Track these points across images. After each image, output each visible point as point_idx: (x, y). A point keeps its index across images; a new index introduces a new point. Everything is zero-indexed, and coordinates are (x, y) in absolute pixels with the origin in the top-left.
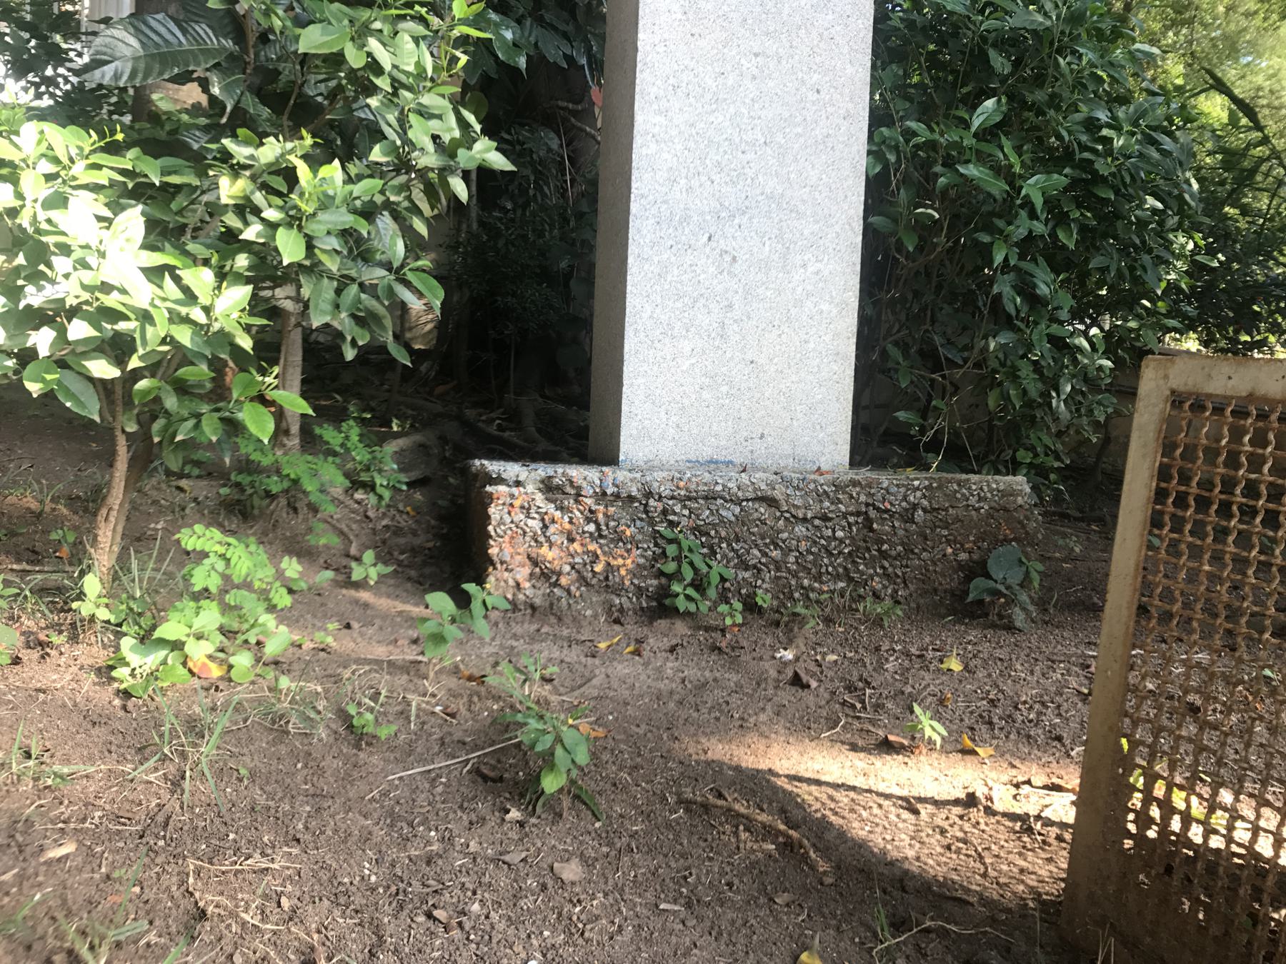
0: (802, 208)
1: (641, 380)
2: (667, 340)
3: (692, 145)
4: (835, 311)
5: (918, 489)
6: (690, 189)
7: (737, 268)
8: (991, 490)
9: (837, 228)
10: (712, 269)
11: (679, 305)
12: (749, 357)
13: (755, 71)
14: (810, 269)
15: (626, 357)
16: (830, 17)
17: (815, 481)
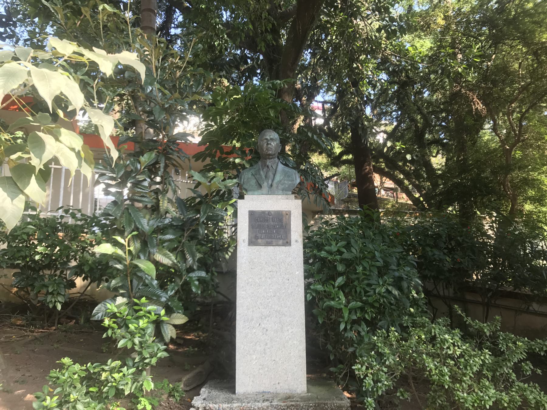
0: (286, 314)
1: (241, 368)
2: (248, 356)
3: (253, 299)
4: (298, 344)
5: (312, 406)
6: (253, 311)
7: (268, 333)
8: (334, 406)
9: (297, 319)
10: (261, 334)
11: (252, 345)
12: (273, 359)
13: (270, 276)
14: (290, 331)
15: (237, 361)
17: (280, 405)
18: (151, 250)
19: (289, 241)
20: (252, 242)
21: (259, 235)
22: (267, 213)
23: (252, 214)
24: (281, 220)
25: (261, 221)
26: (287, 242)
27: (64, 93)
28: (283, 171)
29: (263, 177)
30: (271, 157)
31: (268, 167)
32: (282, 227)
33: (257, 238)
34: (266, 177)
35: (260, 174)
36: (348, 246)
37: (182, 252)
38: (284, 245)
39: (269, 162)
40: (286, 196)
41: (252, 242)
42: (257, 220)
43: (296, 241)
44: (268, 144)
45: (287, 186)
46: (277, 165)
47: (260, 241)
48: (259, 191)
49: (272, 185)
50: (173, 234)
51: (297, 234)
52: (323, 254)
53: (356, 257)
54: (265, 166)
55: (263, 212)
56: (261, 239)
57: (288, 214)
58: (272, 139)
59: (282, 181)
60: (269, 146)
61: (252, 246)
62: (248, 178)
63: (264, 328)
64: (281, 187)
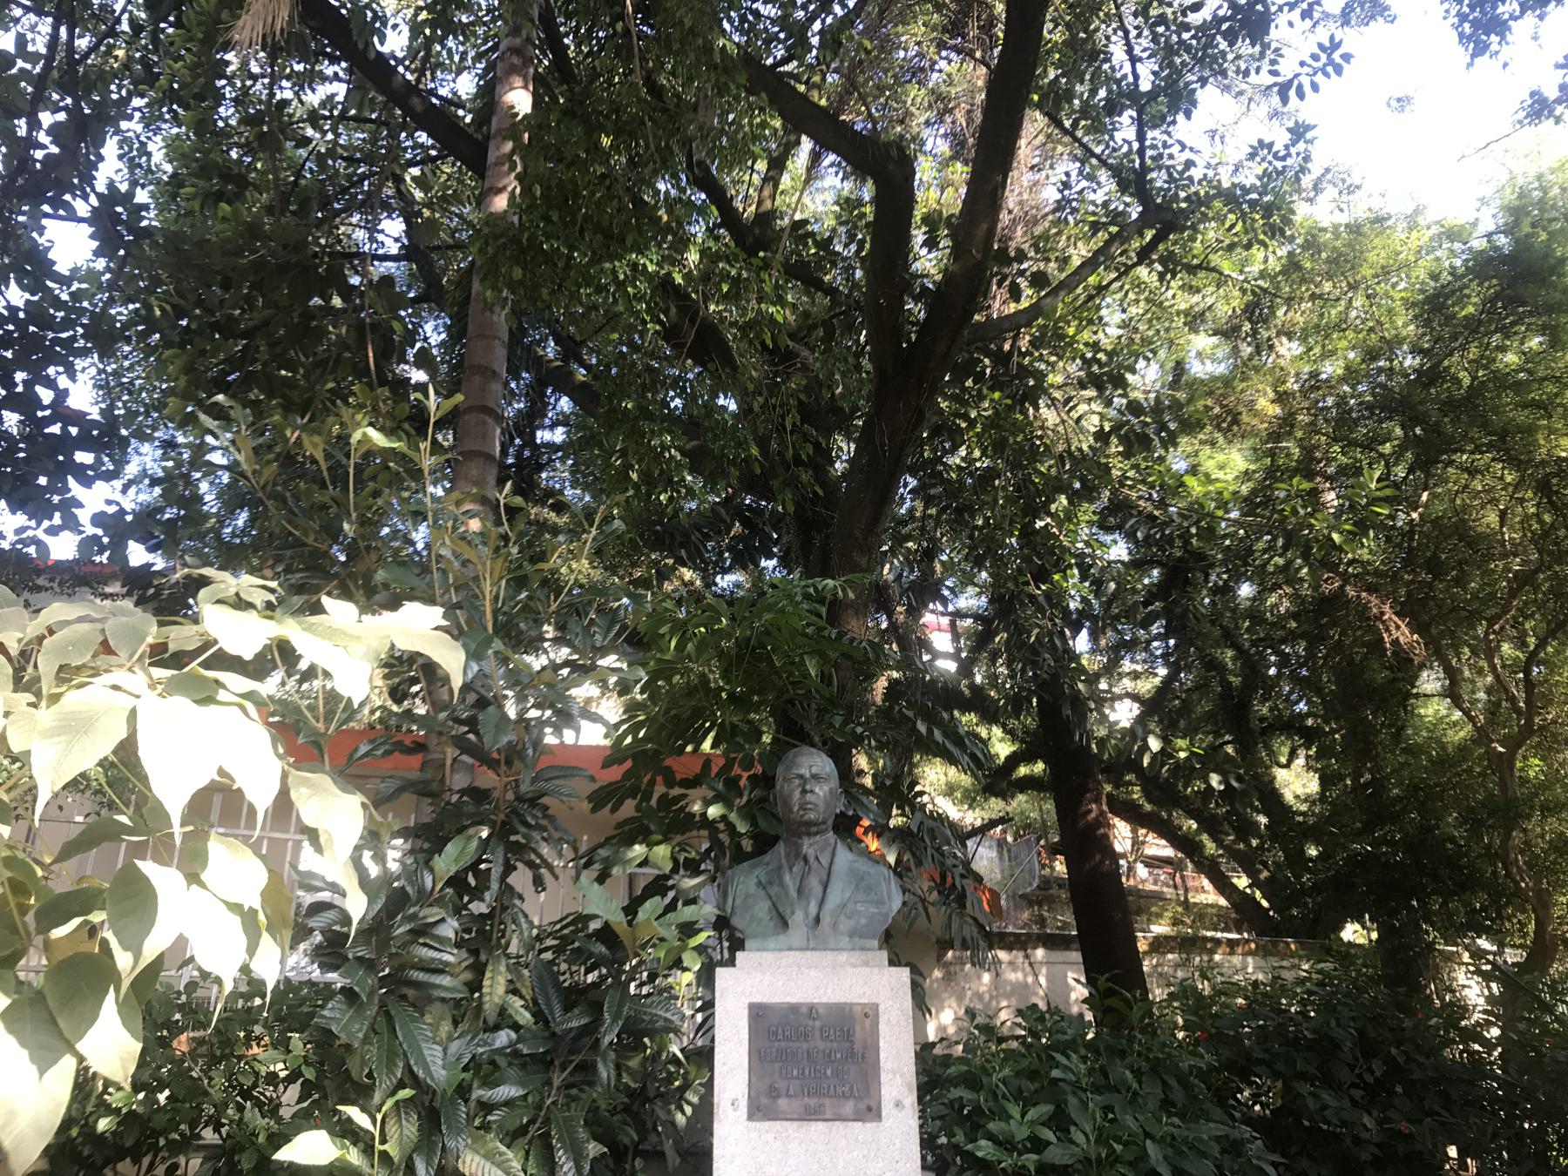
16: (881, 1164)
18: (451, 1144)
19: (874, 1105)
20: (761, 1108)
21: (781, 1085)
22: (804, 1010)
23: (759, 1014)
24: (847, 1035)
25: (786, 1038)
26: (869, 1109)
27: (226, 769)
28: (852, 872)
29: (793, 893)
30: (814, 829)
31: (806, 860)
32: (851, 1055)
33: (773, 1093)
34: (800, 891)
35: (782, 884)
36: (1061, 1122)
37: (546, 1137)
38: (859, 1117)
39: (808, 846)
40: (863, 956)
41: (761, 1108)
42: (776, 1034)
43: (898, 1104)
44: (804, 792)
45: (863, 921)
46: (833, 855)
47: (783, 1103)
48: (782, 938)
49: (817, 920)
50: (521, 1084)
51: (899, 1080)
52: (984, 1149)
53: (1088, 1160)
54: (797, 855)
55: (794, 1008)
56: (788, 1096)
57: (871, 1013)
58: (815, 777)
59: (850, 907)
60: (809, 797)
61: (758, 1120)
62: (747, 896)
64: (846, 924)
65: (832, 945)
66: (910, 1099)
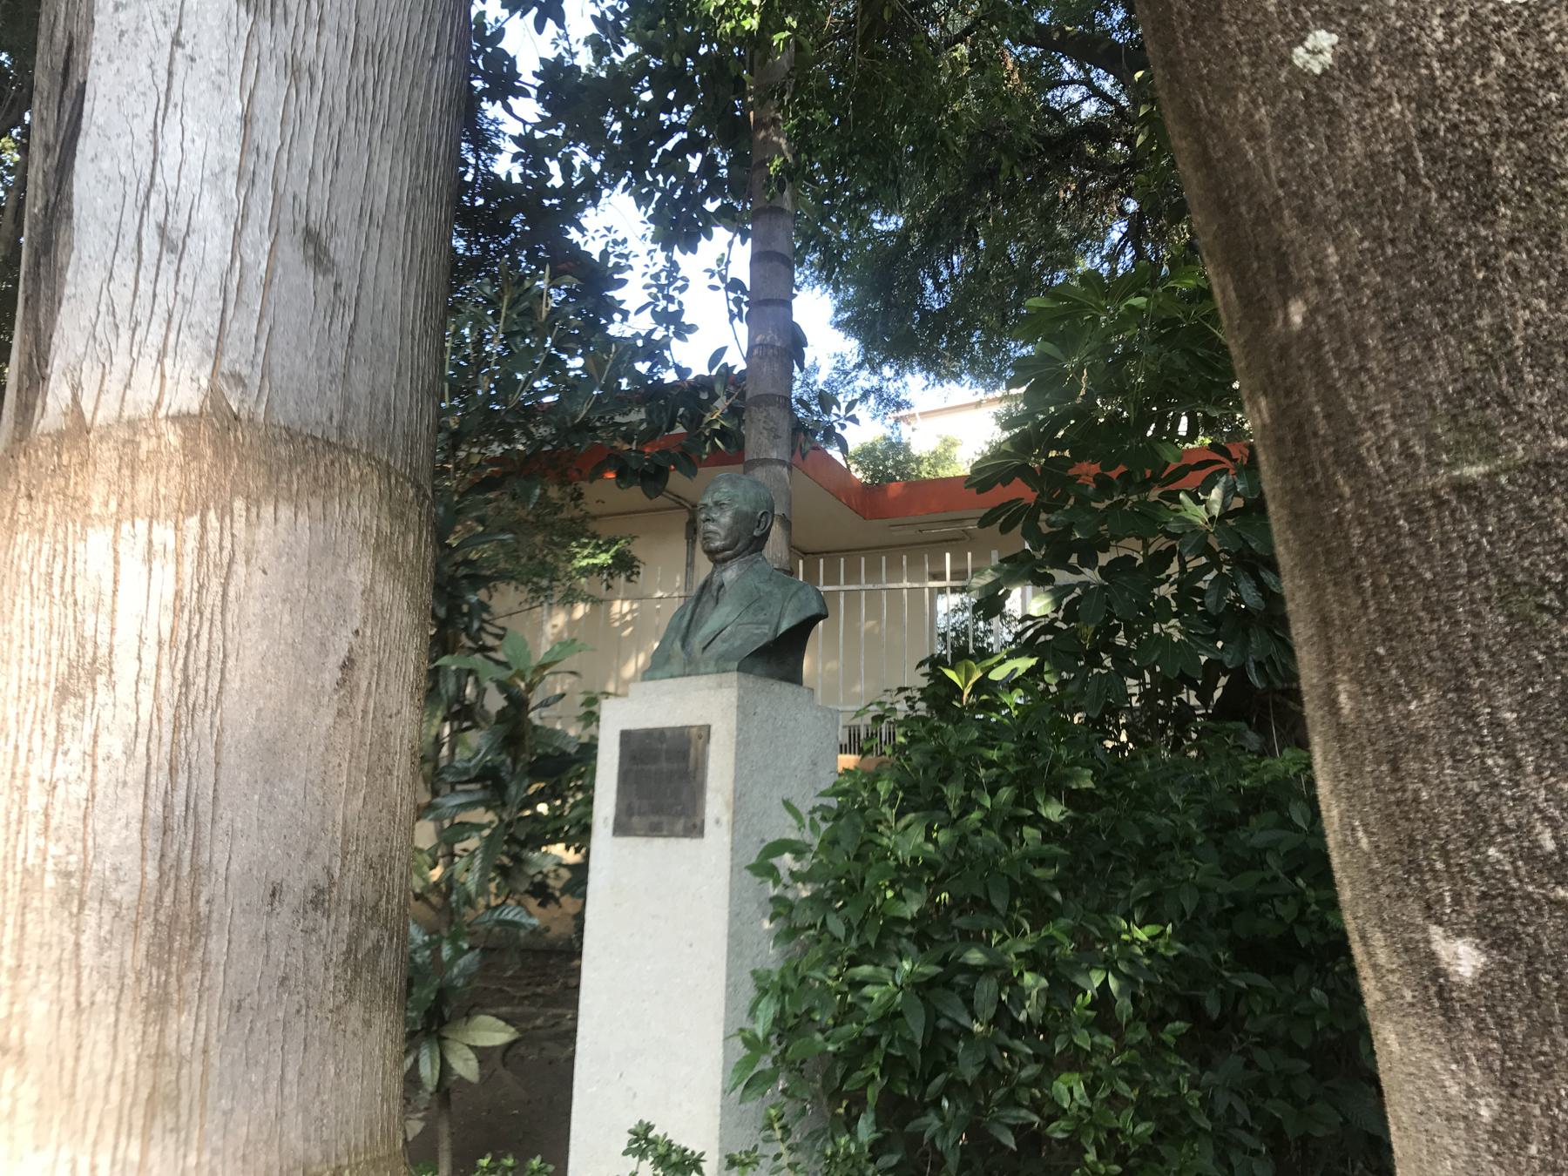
19: (698, 823)
21: (636, 803)
23: (626, 736)
24: (685, 755)
26: (695, 826)
47: (635, 819)
55: (649, 733)
56: (640, 814)
63: (629, 1088)
65: (702, 670)
66: (726, 818)
